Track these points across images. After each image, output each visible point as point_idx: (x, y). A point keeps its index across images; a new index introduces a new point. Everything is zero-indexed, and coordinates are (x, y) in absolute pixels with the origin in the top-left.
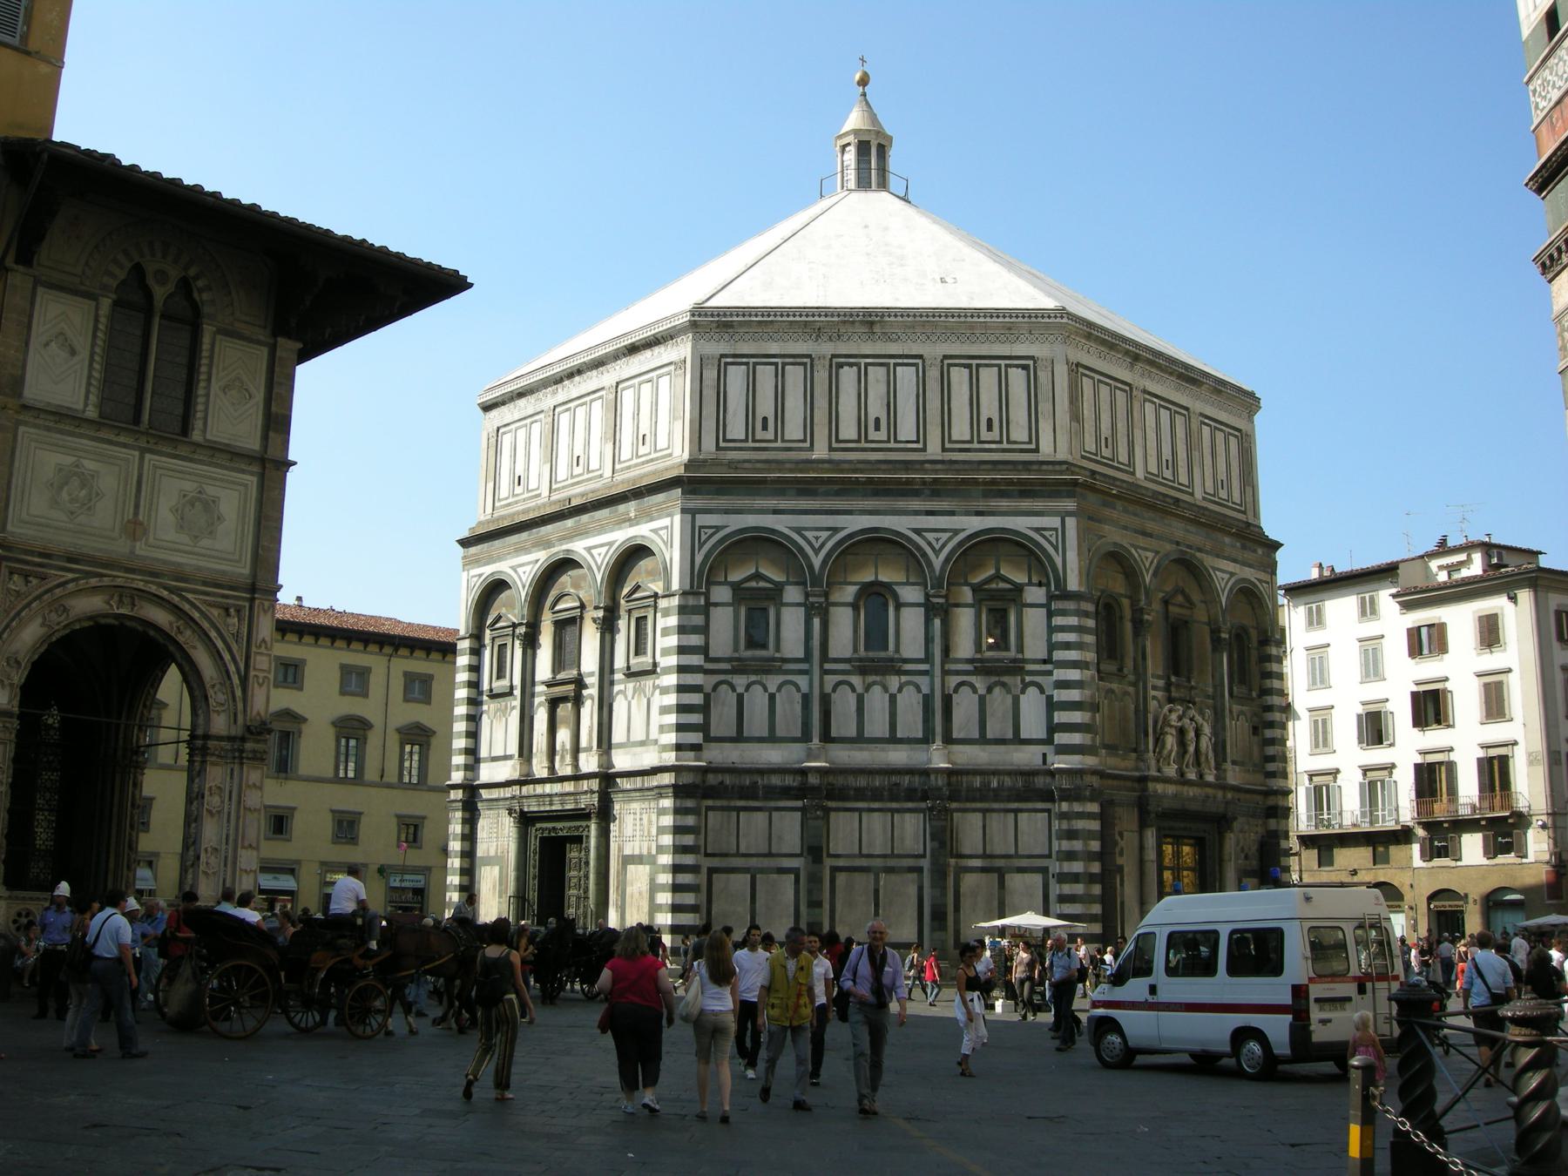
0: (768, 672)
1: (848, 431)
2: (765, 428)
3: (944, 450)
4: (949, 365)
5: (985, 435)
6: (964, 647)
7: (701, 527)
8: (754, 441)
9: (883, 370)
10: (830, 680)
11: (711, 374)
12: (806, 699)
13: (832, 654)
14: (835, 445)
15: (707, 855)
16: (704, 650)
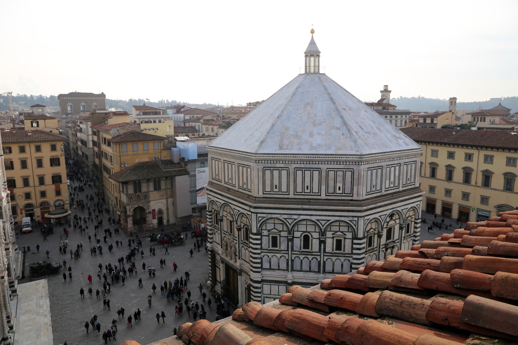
0: (278, 253)
1: (299, 189)
2: (276, 188)
3: (326, 195)
4: (328, 171)
5: (338, 191)
6: (329, 249)
7: (259, 217)
8: (273, 192)
9: (310, 171)
10: (294, 256)
11: (261, 173)
12: (288, 260)
13: (295, 249)
14: (295, 193)
15: (263, 294)
16: (261, 248)
